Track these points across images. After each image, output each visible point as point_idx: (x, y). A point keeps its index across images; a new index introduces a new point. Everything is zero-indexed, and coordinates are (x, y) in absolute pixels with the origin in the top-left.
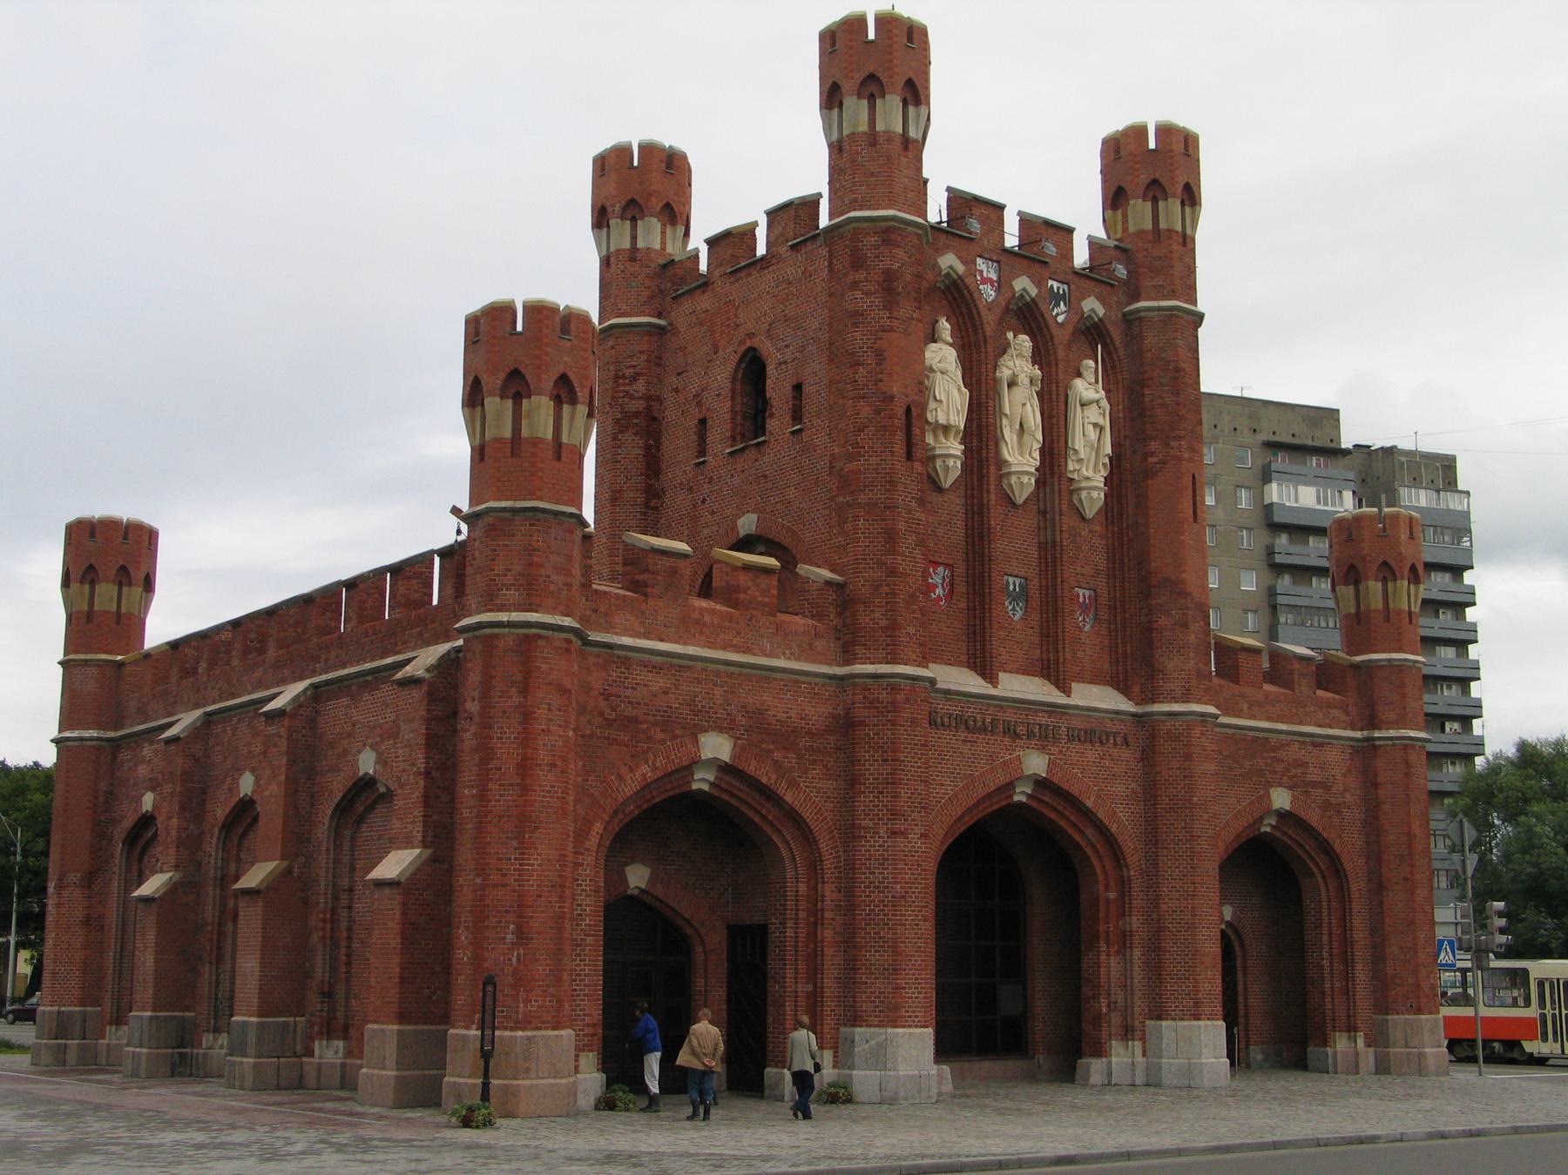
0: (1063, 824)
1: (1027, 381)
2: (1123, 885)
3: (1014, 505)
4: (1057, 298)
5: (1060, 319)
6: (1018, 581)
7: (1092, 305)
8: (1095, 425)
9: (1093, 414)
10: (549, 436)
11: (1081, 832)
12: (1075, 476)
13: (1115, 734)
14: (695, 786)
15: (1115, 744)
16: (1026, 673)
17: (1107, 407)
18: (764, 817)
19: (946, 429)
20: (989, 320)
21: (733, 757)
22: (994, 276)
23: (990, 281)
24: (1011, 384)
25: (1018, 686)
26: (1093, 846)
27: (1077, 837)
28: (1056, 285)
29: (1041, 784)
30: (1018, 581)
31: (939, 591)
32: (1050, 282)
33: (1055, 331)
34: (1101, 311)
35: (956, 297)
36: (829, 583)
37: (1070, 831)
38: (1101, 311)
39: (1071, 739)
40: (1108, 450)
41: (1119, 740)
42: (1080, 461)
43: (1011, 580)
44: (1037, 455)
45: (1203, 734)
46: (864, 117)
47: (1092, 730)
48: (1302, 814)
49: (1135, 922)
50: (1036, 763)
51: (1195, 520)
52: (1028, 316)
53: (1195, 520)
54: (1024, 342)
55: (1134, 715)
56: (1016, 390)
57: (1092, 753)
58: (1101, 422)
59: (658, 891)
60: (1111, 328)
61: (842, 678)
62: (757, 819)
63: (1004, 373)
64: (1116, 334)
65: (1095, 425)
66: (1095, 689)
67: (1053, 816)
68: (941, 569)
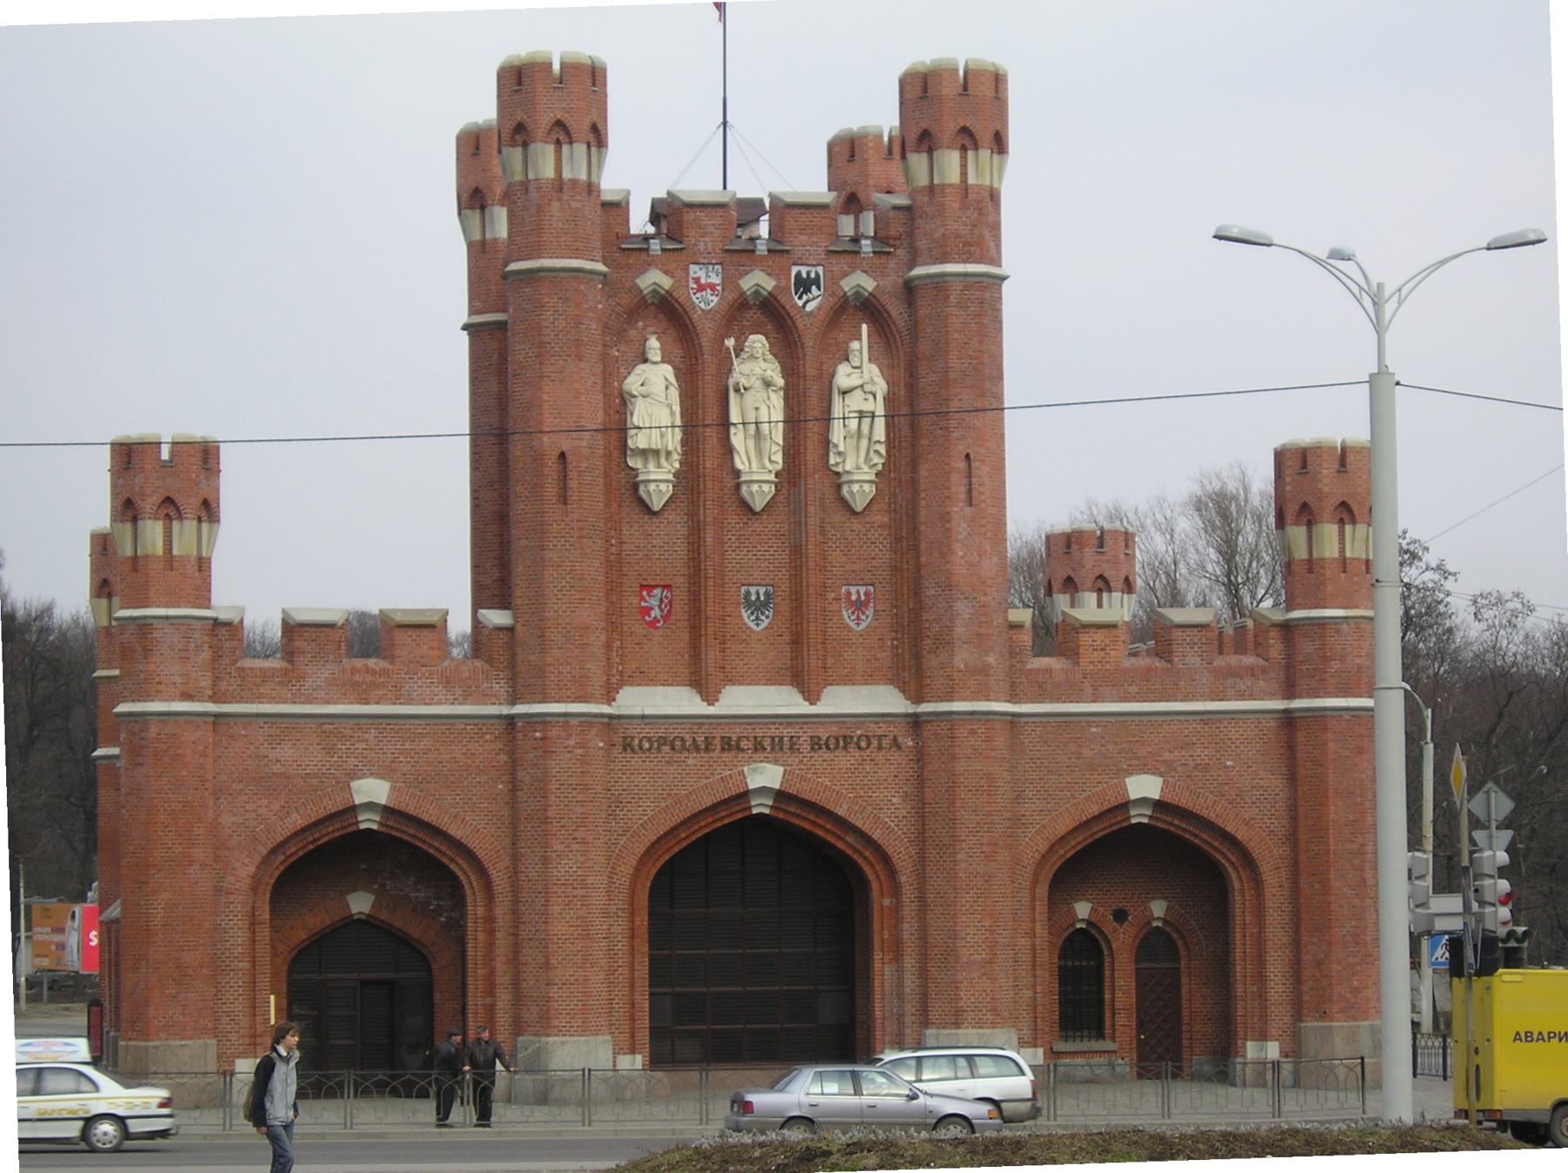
0: (820, 833)
1: (758, 384)
2: (896, 890)
3: (754, 513)
4: (804, 285)
5: (809, 307)
6: (762, 590)
8: (861, 415)
9: (856, 402)
10: (160, 551)
11: (839, 838)
12: (840, 469)
13: (880, 737)
14: (363, 826)
15: (880, 748)
16: (770, 682)
17: (881, 387)
18: (437, 849)
20: (706, 331)
22: (715, 279)
23: (712, 287)
25: (741, 700)
26: (861, 854)
27: (840, 845)
28: (804, 271)
29: (781, 796)
30: (762, 590)
31: (656, 613)
32: (794, 270)
33: (800, 323)
34: (868, 284)
35: (670, 312)
36: (499, 629)
37: (829, 838)
39: (816, 744)
41: (885, 743)
42: (840, 453)
43: (753, 590)
44: (779, 458)
45: (972, 732)
46: (518, 165)
47: (846, 735)
48: (1185, 801)
49: (908, 929)
50: (766, 776)
52: (772, 315)
54: (757, 342)
55: (907, 715)
56: (749, 396)
57: (844, 760)
58: (868, 406)
59: (384, 915)
60: (885, 299)
61: (511, 719)
62: (432, 851)
63: (731, 382)
64: (896, 310)
66: (864, 690)
67: (807, 826)
68: (657, 591)
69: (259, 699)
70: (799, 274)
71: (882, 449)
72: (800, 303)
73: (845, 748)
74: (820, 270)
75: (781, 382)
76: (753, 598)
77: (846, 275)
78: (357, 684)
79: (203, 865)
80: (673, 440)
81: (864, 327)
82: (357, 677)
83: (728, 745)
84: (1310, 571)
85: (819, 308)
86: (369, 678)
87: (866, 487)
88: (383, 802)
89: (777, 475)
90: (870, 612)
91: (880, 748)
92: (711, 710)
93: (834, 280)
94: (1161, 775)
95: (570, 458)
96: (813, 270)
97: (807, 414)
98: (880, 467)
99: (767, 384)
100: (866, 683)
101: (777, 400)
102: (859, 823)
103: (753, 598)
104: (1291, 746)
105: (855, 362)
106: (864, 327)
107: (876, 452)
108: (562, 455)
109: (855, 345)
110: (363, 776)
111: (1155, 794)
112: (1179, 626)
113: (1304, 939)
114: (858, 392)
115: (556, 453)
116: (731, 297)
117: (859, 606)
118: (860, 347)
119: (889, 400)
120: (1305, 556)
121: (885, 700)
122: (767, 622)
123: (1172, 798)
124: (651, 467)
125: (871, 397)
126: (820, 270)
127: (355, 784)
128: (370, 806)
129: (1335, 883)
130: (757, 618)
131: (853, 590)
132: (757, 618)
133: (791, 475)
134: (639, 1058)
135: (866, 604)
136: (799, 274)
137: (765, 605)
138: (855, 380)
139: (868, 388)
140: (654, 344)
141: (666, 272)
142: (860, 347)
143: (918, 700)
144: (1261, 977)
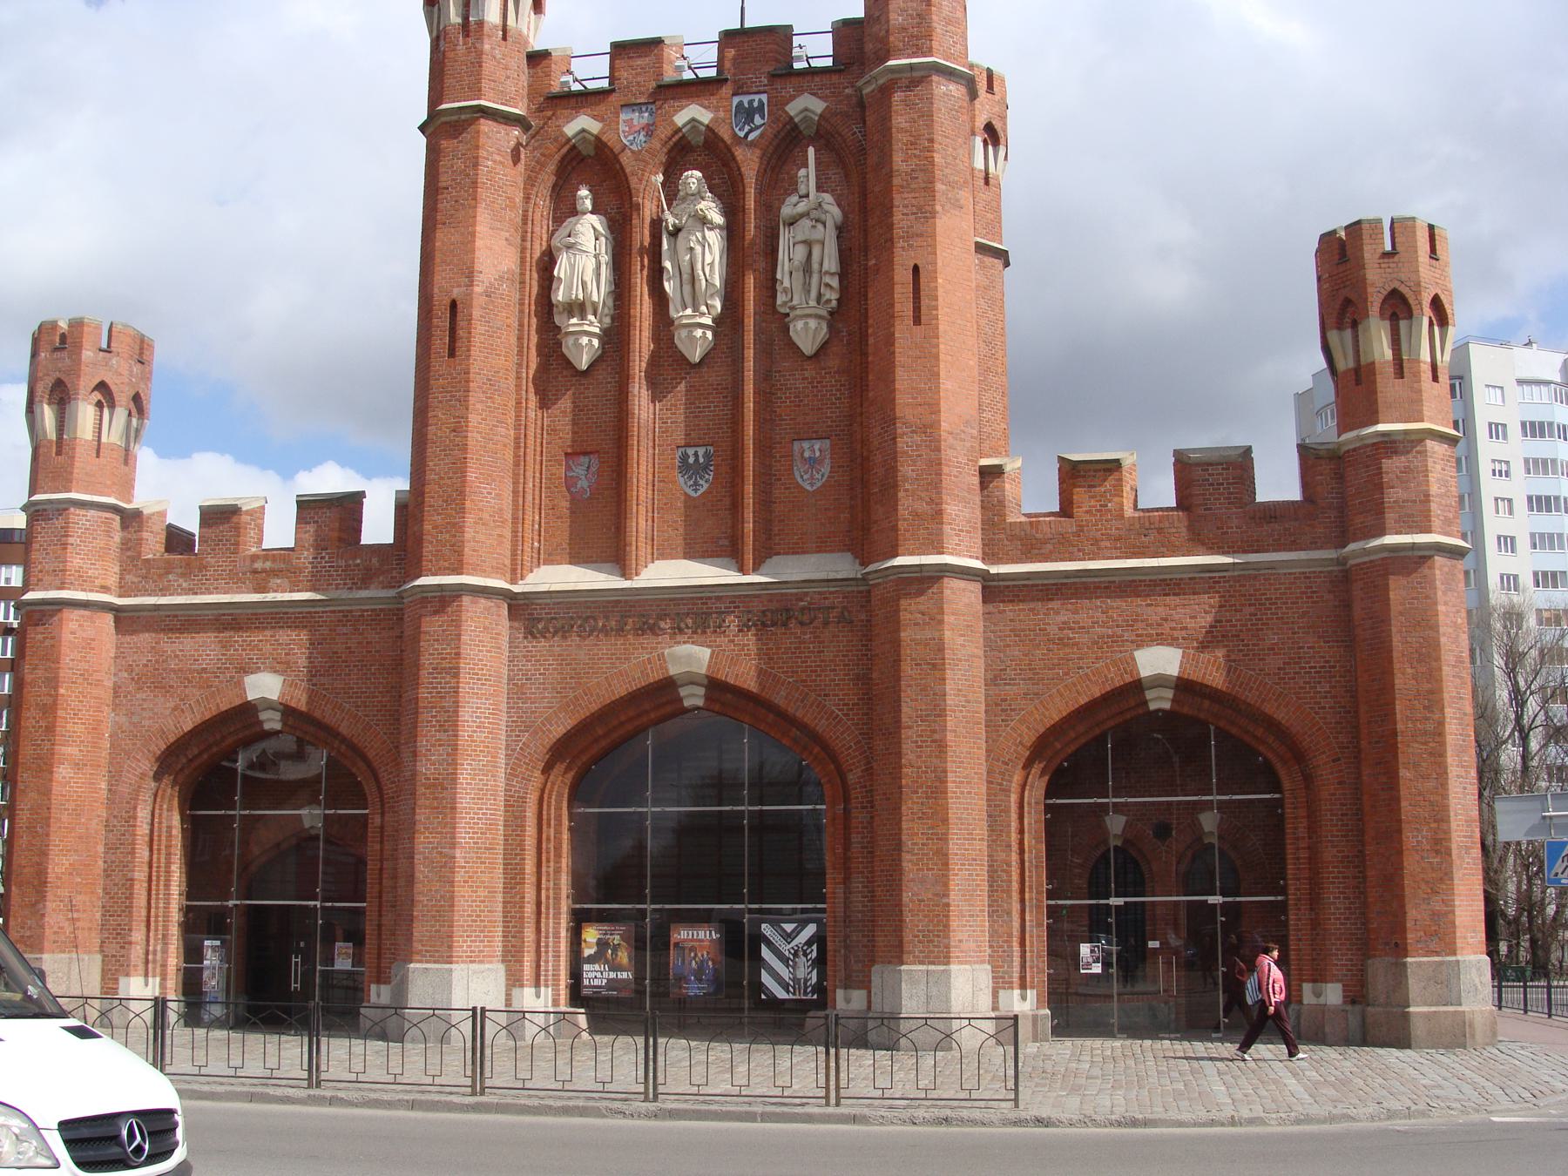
6: (701, 451)
7: (806, 105)
8: (808, 244)
9: (804, 229)
17: (834, 212)
19: (578, 308)
21: (283, 694)
24: (676, 232)
28: (745, 99)
30: (701, 451)
32: (736, 100)
38: (817, 106)
40: (831, 263)
42: (785, 291)
51: (917, 320)
53: (917, 320)
65: (808, 244)
69: (164, 591)
70: (741, 103)
71: (835, 282)
72: (742, 134)
73: (785, 624)
74: (764, 97)
75: (718, 219)
76: (691, 460)
77: (793, 98)
78: (255, 572)
79: (77, 766)
80: (599, 292)
81: (811, 150)
82: (258, 565)
83: (648, 628)
84: (1358, 382)
85: (762, 135)
86: (268, 565)
87: (813, 323)
88: (275, 697)
89: (714, 320)
90: (826, 469)
91: (826, 624)
92: (626, 584)
93: (778, 104)
94: (1178, 646)
95: (460, 306)
96: (756, 97)
97: (750, 254)
98: (834, 303)
99: (704, 221)
100: (819, 550)
101: (715, 239)
102: (799, 714)
103: (691, 460)
104: (1347, 605)
105: (802, 191)
106: (811, 150)
107: (827, 285)
108: (454, 304)
109: (802, 172)
110: (258, 670)
111: (1173, 670)
112: (1198, 465)
113: (1369, 849)
114: (806, 223)
115: (447, 301)
116: (663, 132)
117: (813, 463)
118: (808, 176)
119: (841, 230)
120: (1351, 364)
121: (838, 566)
122: (706, 486)
123: (1196, 676)
124: (574, 321)
125: (820, 226)
126: (764, 97)
127: (250, 680)
128: (268, 704)
129: (1404, 773)
130: (696, 483)
131: (806, 445)
132: (696, 483)
133: (728, 322)
134: (547, 993)
135: (820, 461)
136: (741, 103)
137: (705, 468)
138: (802, 207)
139: (814, 214)
140: (584, 192)
141: (594, 117)
142: (808, 176)
143: (864, 564)
144: (1314, 900)
